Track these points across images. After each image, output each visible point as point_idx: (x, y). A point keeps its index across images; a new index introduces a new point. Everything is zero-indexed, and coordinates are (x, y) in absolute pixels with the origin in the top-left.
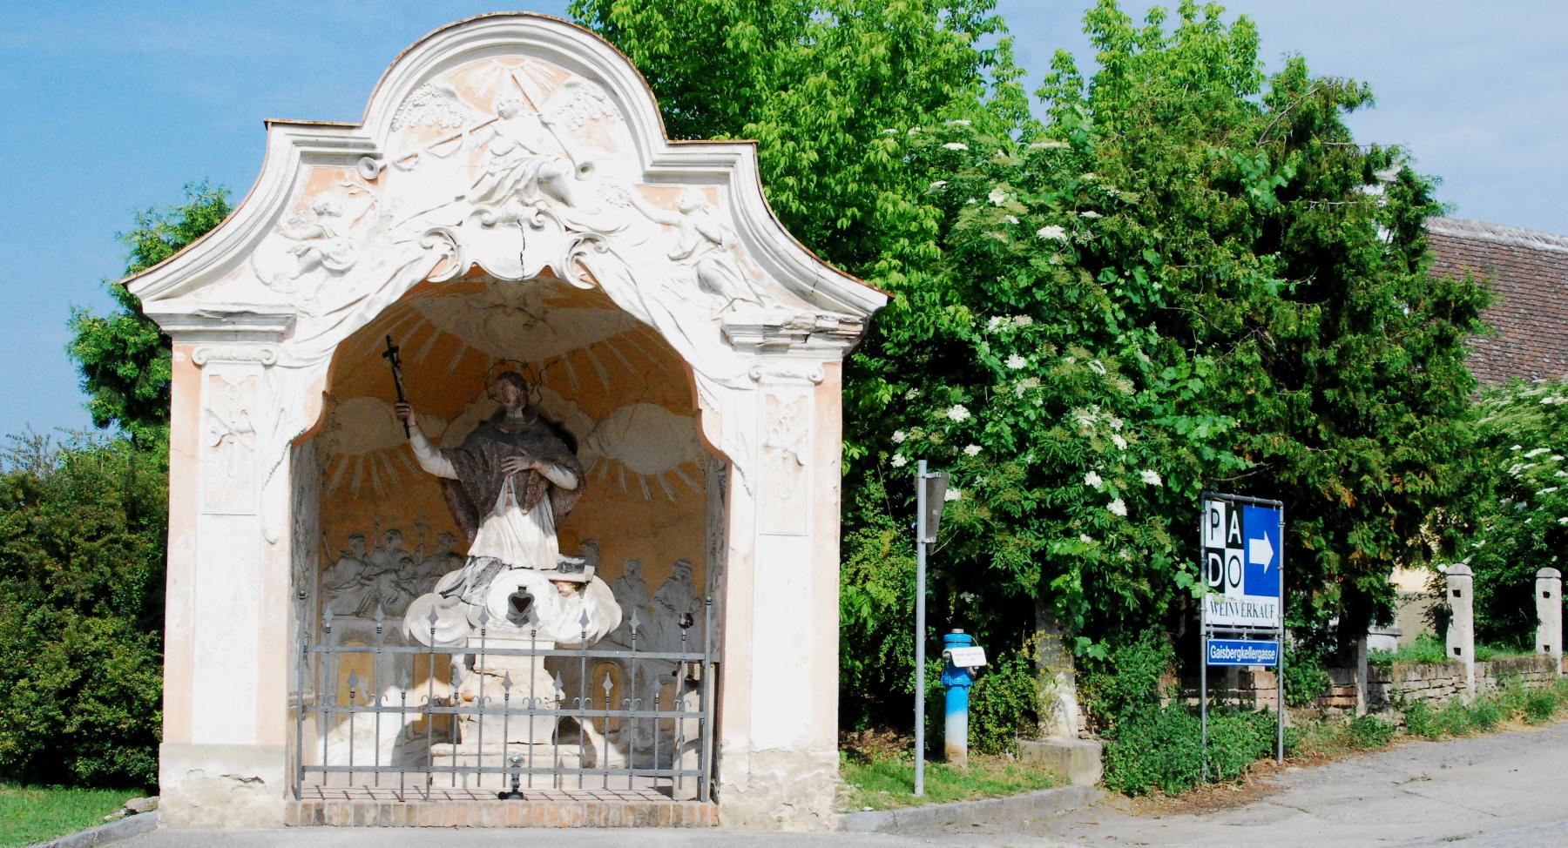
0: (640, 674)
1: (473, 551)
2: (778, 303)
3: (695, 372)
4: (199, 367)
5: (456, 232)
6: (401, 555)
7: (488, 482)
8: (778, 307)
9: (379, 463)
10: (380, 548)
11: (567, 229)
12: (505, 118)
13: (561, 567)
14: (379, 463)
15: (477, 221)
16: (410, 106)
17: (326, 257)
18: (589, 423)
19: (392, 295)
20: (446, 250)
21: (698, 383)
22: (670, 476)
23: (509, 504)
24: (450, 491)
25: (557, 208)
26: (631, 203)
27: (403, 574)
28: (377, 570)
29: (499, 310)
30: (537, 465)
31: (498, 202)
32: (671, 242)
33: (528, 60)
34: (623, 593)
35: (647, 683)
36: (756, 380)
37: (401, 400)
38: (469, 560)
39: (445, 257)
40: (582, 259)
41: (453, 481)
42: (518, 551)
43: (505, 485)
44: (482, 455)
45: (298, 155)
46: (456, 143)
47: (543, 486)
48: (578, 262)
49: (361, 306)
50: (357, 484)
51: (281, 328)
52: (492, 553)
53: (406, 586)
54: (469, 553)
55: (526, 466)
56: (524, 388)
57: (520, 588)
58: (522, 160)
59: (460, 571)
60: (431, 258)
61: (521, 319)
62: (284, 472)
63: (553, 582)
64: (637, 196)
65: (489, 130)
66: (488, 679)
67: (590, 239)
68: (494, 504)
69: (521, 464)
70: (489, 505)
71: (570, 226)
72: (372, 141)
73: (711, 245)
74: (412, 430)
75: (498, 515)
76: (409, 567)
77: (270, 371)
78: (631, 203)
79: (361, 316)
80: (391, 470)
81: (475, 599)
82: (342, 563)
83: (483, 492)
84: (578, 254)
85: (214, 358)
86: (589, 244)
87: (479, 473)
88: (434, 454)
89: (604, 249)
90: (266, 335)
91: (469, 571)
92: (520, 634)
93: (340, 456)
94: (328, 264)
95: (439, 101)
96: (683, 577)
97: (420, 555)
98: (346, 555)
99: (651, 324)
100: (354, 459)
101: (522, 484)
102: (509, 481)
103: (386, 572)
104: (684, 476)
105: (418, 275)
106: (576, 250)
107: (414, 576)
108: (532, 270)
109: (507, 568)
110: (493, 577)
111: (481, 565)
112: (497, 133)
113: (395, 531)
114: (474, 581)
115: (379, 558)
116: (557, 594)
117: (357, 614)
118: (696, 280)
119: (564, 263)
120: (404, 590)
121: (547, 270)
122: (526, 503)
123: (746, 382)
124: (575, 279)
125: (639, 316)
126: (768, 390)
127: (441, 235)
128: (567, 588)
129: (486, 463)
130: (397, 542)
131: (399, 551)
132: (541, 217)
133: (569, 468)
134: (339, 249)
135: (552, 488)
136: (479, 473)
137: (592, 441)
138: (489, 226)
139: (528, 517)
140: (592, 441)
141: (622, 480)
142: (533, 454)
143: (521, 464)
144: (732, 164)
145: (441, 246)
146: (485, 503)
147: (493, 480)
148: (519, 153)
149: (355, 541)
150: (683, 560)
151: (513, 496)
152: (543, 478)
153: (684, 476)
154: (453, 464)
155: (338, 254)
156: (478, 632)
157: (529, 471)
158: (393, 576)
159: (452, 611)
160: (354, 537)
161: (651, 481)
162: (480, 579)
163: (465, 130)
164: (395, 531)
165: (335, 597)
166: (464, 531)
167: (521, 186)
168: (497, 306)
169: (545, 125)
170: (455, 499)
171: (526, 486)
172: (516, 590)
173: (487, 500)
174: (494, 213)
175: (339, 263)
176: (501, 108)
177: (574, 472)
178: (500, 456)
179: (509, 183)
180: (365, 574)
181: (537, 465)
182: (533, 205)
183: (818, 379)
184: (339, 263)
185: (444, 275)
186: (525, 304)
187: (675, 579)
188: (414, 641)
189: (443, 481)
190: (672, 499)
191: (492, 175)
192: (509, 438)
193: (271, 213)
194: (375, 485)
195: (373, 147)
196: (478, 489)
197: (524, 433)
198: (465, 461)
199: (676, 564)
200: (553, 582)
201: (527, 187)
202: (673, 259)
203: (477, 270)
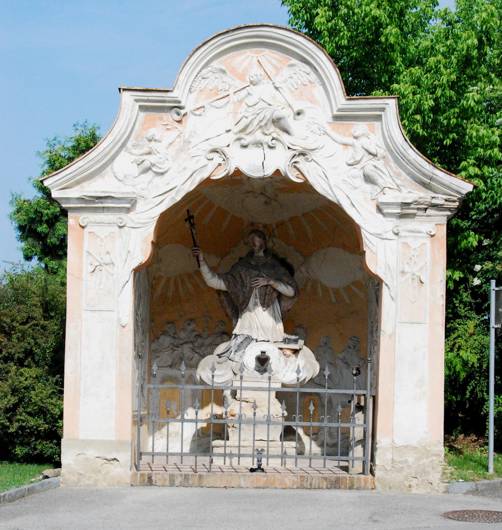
0: (330, 402)
1: (236, 331)
2: (410, 190)
3: (361, 229)
4: (83, 227)
5: (226, 150)
6: (196, 333)
7: (244, 292)
8: (410, 192)
9: (183, 282)
10: (183, 329)
11: (289, 148)
12: (254, 85)
13: (285, 341)
15: (238, 144)
16: (200, 79)
17: (153, 165)
18: (301, 259)
19: (190, 187)
20: (220, 161)
21: (363, 236)
22: (347, 289)
23: (256, 304)
24: (223, 297)
25: (284, 137)
26: (326, 133)
27: (196, 344)
28: (182, 342)
29: (251, 194)
30: (272, 283)
31: (250, 133)
32: (348, 155)
33: (267, 51)
34: (320, 356)
35: (334, 406)
36: (397, 234)
37: (195, 246)
38: (233, 336)
39: (220, 165)
40: (297, 165)
41: (224, 292)
42: (261, 331)
43: (254, 294)
45: (137, 107)
46: (226, 100)
47: (275, 295)
48: (295, 167)
49: (173, 193)
50: (170, 293)
51: (128, 206)
52: (246, 332)
53: (197, 351)
54: (233, 333)
55: (265, 283)
56: (264, 239)
57: (262, 352)
58: (263, 109)
59: (229, 342)
60: (211, 166)
61: (263, 199)
62: (130, 285)
63: (281, 349)
64: (329, 129)
65: (244, 92)
66: (244, 404)
67: (302, 154)
68: (247, 305)
69: (262, 282)
71: (291, 146)
72: (179, 99)
73: (371, 157)
74: (202, 263)
75: (250, 311)
76: (200, 341)
77: (122, 230)
78: (326, 133)
79: (173, 198)
80: (190, 286)
81: (237, 358)
82: (162, 337)
83: (241, 299)
84: (295, 162)
85: (91, 222)
86: (301, 157)
87: (239, 287)
88: (213, 276)
89: (310, 159)
90: (120, 210)
91: (233, 343)
92: (262, 378)
93: (161, 277)
94: (154, 169)
95: (217, 75)
96: (354, 347)
97: (205, 334)
98: (165, 333)
99: (336, 202)
100: (168, 280)
101: (263, 293)
102: (256, 292)
103: (186, 343)
104: (354, 288)
105: (205, 175)
106: (294, 160)
107: (202, 345)
108: (269, 172)
109: (255, 341)
110: (247, 346)
111: (240, 340)
112: (249, 94)
113: (192, 320)
114: (236, 348)
115: (183, 335)
116: (283, 356)
117: (171, 366)
118: (362, 177)
119: (287, 168)
120: (196, 352)
121: (278, 172)
122: (266, 304)
123: (391, 235)
124: (294, 176)
125: (330, 198)
126: (404, 240)
127: (217, 152)
128: (288, 352)
129: (243, 281)
130: (193, 326)
131: (194, 331)
132: (274, 141)
133: (290, 285)
134: (160, 161)
135: (280, 296)
136: (239, 287)
137: (303, 269)
138: (244, 147)
139: (266, 312)
140: (303, 269)
141: (320, 290)
142: (270, 277)
143: (262, 282)
144: (383, 110)
145: (217, 159)
147: (247, 291)
148: (262, 105)
149: (169, 325)
150: (355, 337)
152: (275, 290)
153: (354, 288)
154: (224, 282)
155: (160, 163)
156: (238, 377)
157: (267, 286)
158: (191, 346)
159: (224, 365)
160: (169, 323)
161: (336, 292)
162: (239, 347)
163: (231, 92)
164: (192, 320)
165: (158, 357)
166: (230, 320)
167: (263, 124)
168: (250, 192)
169: (277, 88)
170: (225, 303)
171: (266, 294)
172: (260, 353)
173: (243, 302)
174: (248, 140)
175: (160, 168)
176: (252, 79)
177: (292, 287)
178: (251, 278)
179: (256, 122)
180: (175, 344)
181: (272, 283)
182: (270, 134)
183: (433, 233)
184: (160, 168)
185: (219, 175)
186: (265, 191)
187: (349, 347)
188: (202, 382)
189: (219, 292)
190: (348, 302)
191: (247, 118)
192: (256, 267)
193: (122, 141)
194: (181, 294)
195: (180, 102)
196: (239, 296)
197: (265, 264)
198: (231, 281)
199: (351, 339)
200: (281, 349)
201: (266, 124)
202: (349, 165)
203: (238, 172)
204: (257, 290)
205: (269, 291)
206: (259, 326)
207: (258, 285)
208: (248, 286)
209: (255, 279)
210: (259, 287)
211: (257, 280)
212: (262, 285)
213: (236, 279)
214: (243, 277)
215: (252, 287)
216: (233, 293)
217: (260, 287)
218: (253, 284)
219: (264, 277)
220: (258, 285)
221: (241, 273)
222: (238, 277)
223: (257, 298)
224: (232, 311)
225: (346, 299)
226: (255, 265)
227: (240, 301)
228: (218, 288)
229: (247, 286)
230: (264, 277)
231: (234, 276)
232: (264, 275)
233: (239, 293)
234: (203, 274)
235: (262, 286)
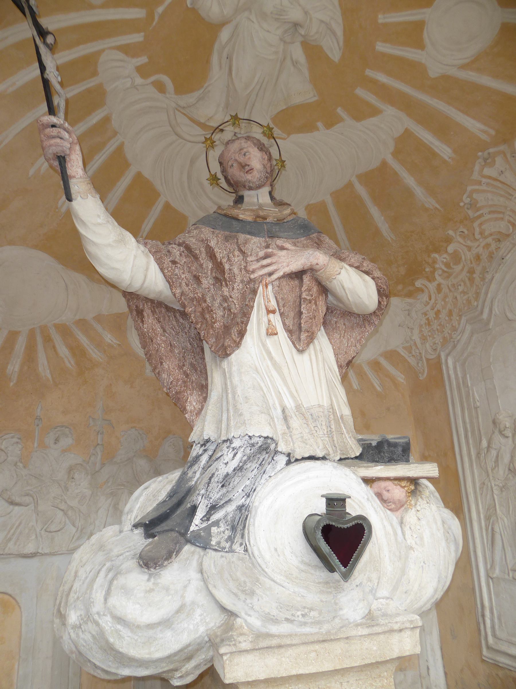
7: (225, 299)
14: (48, 340)
22: (376, 365)
43: (259, 299)
44: (212, 256)
70: (234, 331)
80: (63, 351)
87: (207, 282)
101: (291, 297)
129: (219, 266)
136: (207, 282)
146: (227, 329)
147: (236, 294)
151: (276, 320)
154: (160, 262)
173: (227, 329)
190: (379, 389)
204: (270, 287)
205: (309, 290)
206: (290, 404)
207: (270, 274)
208: (238, 279)
209: (261, 254)
210: (275, 276)
211: (267, 256)
212: (288, 270)
213: (196, 258)
214: (219, 256)
215: (251, 280)
216: (192, 300)
217: (279, 278)
218: (253, 272)
219: (286, 249)
220: (270, 274)
221: (212, 244)
222: (204, 255)
223: (274, 312)
224: (180, 367)
225: (375, 385)
226: (255, 222)
227: (217, 325)
228: (136, 286)
229: (233, 279)
230: (286, 249)
231: (188, 248)
232: (287, 245)
233: (208, 300)
234: (82, 230)
235: (284, 276)
